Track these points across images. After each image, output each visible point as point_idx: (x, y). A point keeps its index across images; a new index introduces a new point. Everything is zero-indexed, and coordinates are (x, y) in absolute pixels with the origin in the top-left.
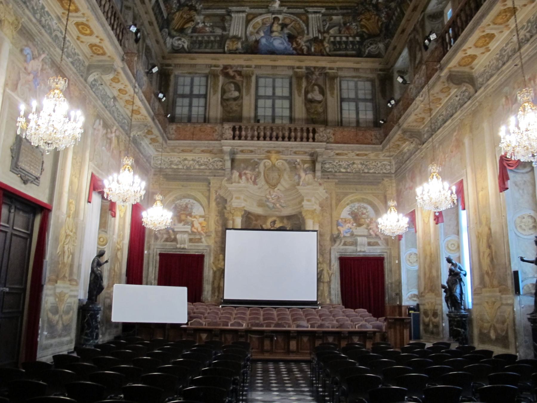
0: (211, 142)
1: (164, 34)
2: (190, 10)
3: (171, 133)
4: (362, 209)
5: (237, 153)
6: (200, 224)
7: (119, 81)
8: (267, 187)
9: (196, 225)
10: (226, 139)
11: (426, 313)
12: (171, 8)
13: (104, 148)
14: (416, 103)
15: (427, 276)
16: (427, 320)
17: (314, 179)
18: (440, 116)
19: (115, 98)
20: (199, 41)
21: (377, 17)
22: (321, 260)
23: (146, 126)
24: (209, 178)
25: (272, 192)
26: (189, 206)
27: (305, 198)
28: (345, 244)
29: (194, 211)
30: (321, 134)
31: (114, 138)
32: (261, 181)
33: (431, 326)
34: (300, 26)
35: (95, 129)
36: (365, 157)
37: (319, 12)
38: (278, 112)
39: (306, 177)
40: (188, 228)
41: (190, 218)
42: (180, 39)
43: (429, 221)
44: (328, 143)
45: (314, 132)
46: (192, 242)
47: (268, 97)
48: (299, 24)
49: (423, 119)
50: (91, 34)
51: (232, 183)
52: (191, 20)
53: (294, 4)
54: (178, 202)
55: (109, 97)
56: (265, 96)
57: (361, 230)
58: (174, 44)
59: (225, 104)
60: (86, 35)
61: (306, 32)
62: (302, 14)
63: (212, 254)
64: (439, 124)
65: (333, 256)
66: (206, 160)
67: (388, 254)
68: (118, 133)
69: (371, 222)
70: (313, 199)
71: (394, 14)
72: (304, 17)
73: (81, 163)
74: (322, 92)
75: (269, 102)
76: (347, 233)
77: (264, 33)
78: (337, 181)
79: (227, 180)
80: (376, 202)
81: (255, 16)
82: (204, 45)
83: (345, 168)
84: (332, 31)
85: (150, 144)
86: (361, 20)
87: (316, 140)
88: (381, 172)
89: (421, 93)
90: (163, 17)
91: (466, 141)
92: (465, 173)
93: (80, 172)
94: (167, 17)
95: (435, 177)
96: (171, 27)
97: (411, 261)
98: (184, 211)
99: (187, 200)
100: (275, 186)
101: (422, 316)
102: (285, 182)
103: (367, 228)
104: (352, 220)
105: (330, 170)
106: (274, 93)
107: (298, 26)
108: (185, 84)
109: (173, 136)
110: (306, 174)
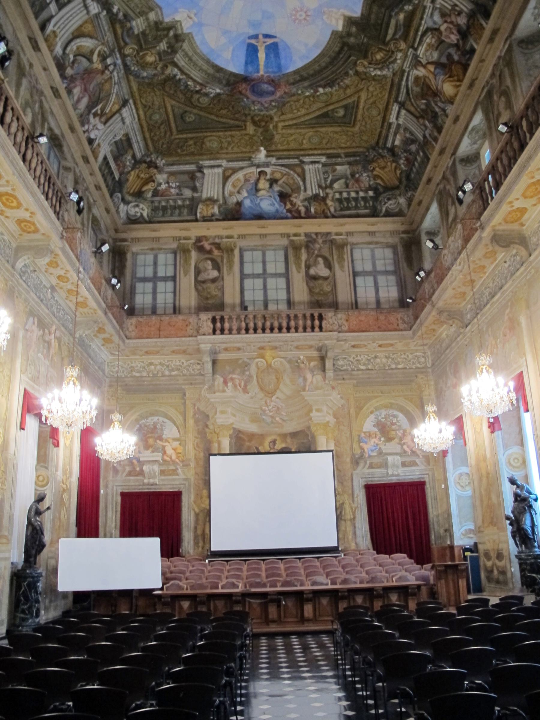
0: (183, 339)
1: (116, 200)
2: (149, 167)
3: (130, 329)
4: (391, 418)
5: (220, 352)
6: (175, 449)
7: (58, 265)
8: (261, 395)
9: (169, 451)
10: (204, 335)
11: (487, 555)
12: (124, 166)
13: (40, 354)
14: (452, 274)
15: (485, 503)
16: (489, 564)
17: (325, 381)
18: (485, 289)
19: (53, 288)
20: (163, 207)
21: (394, 165)
22: (340, 490)
23: (95, 322)
24: (183, 387)
25: (268, 401)
26: (158, 426)
27: (314, 408)
28: (371, 467)
29: (165, 432)
30: (330, 320)
31: (53, 341)
32: (254, 387)
33: (496, 572)
34: (294, 180)
35: (27, 330)
36: (390, 348)
37: (318, 162)
38: (272, 295)
39: (314, 379)
40: (158, 456)
41: (161, 443)
42: (137, 206)
43: (481, 429)
44: (339, 332)
45: (321, 318)
46: (165, 475)
47: (258, 276)
48: (292, 178)
49: (464, 293)
50: (19, 205)
51: (215, 393)
52: (151, 179)
53: (285, 153)
54: (143, 421)
55: (45, 287)
56: (253, 274)
57: (392, 447)
58: (129, 212)
59: (200, 288)
60: (12, 208)
61: (302, 188)
62: (296, 165)
63: (192, 490)
64: (485, 300)
65: (356, 484)
66: (178, 363)
67: (431, 476)
68: (58, 334)
69: (404, 435)
70: (325, 408)
71: (416, 159)
72: (299, 170)
73: (10, 377)
74: (329, 265)
75: (259, 282)
76: (372, 451)
77: (247, 191)
78: (355, 382)
79: (207, 389)
80: (410, 407)
81: (235, 171)
82: (169, 211)
83: (364, 364)
84: (336, 186)
85: (103, 345)
86: (374, 169)
87: (324, 330)
88: (414, 367)
89: (459, 260)
90: (114, 178)
91: (523, 320)
92: (525, 363)
93: (9, 388)
94: (120, 179)
95: (484, 371)
96: (125, 191)
97: (462, 484)
98: (151, 433)
99: (155, 419)
100: (270, 394)
101: (483, 560)
102: (286, 389)
103: (399, 444)
104: (378, 433)
105: (345, 368)
106: (265, 270)
107: (291, 182)
108: (147, 263)
109: (133, 334)
110: (313, 376)
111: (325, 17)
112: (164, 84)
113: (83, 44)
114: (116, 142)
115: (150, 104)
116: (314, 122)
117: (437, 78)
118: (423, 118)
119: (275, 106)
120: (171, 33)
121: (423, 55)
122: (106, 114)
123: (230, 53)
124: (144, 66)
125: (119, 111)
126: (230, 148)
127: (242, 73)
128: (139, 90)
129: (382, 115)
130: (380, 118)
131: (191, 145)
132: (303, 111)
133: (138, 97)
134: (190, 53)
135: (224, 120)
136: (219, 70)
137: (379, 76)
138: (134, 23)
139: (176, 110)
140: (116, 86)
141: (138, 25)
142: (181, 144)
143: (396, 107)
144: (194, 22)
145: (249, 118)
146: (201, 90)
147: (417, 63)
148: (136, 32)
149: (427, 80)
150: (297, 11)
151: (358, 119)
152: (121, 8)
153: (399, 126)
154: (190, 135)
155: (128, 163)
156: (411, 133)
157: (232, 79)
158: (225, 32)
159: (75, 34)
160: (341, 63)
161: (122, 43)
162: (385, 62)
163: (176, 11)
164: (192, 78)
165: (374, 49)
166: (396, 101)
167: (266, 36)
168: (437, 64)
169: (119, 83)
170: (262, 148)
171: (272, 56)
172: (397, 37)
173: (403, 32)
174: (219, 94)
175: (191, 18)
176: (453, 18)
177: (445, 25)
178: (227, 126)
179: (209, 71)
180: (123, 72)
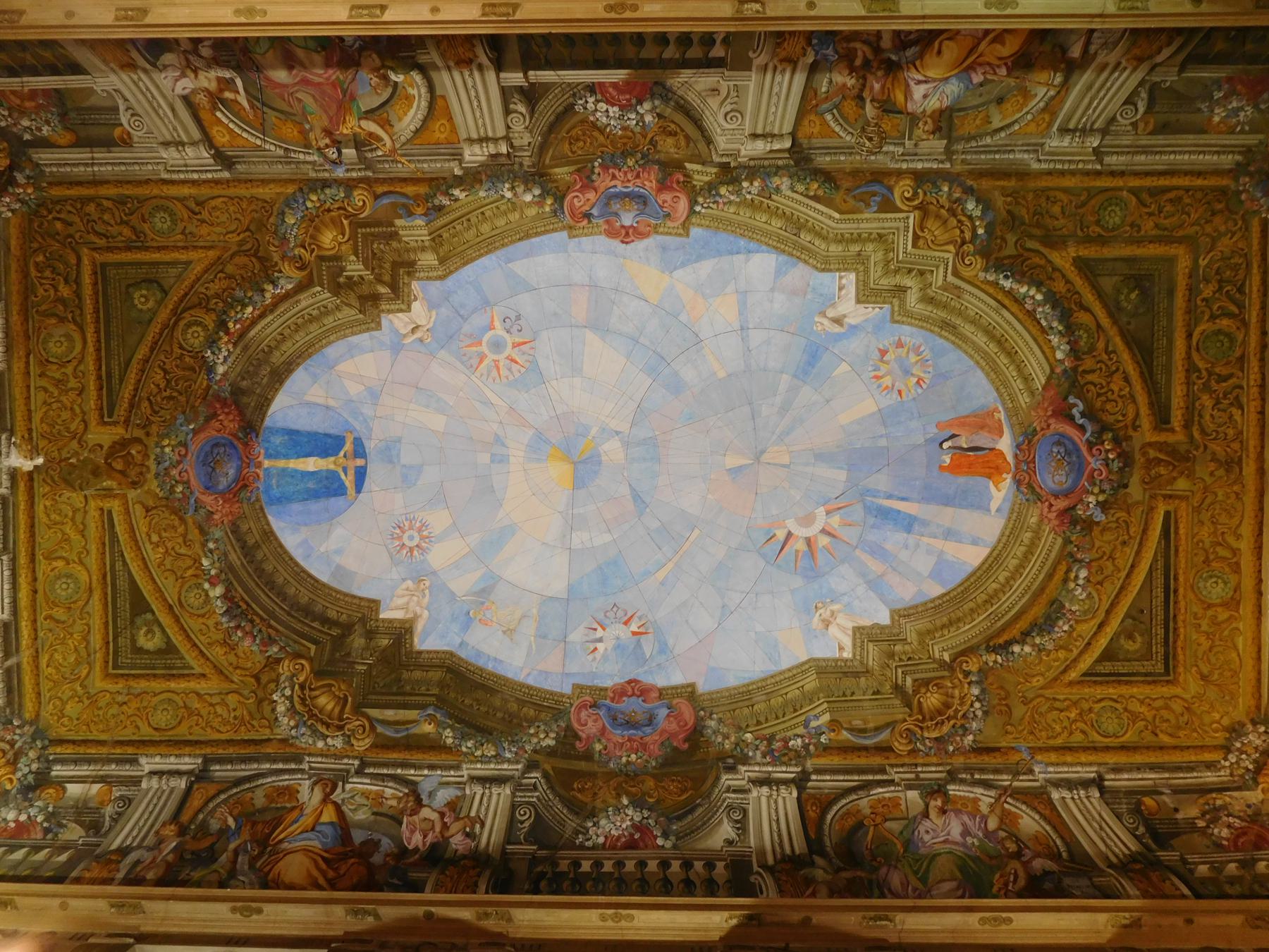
53: (22, 518)
71: (37, 849)
111: (409, 583)
112: (255, 255)
113: (412, 111)
114: (116, 109)
115: (205, 215)
116: (122, 584)
117: (310, 835)
118: (182, 831)
119: (172, 491)
120: (383, 290)
121: (352, 790)
122: (215, 108)
123: (321, 401)
124: (313, 222)
125: (208, 140)
126: (43, 382)
127: (268, 422)
128: (253, 199)
129: (157, 736)
130: (146, 732)
131: (56, 290)
132: (154, 556)
133: (231, 192)
134: (329, 321)
135: (132, 376)
136: (279, 376)
137: (274, 710)
139: (173, 271)
140: (281, 152)
141: (414, 230)
143: (189, 763)
144: (405, 336)
145: (138, 433)
146: (227, 332)
147: (329, 783)
149: (295, 814)
150: (420, 530)
151: (132, 683)
152: (458, 204)
153: (136, 781)
154: (87, 291)
155: (26, 123)
156: (117, 818)
157: (250, 401)
158: (374, 396)
159: (440, 102)
160: (298, 626)
161: (380, 189)
162: (312, 716)
163: (432, 306)
165: (341, 688)
166: (207, 761)
167: (361, 475)
168: (343, 826)
169: (286, 160)
170: (40, 461)
171: (311, 485)
172: (380, 729)
173: (395, 739)
174: (211, 370)
175: (413, 330)
176: (455, 827)
177: (434, 816)
178: (116, 380)
179: (277, 354)
180: (313, 175)
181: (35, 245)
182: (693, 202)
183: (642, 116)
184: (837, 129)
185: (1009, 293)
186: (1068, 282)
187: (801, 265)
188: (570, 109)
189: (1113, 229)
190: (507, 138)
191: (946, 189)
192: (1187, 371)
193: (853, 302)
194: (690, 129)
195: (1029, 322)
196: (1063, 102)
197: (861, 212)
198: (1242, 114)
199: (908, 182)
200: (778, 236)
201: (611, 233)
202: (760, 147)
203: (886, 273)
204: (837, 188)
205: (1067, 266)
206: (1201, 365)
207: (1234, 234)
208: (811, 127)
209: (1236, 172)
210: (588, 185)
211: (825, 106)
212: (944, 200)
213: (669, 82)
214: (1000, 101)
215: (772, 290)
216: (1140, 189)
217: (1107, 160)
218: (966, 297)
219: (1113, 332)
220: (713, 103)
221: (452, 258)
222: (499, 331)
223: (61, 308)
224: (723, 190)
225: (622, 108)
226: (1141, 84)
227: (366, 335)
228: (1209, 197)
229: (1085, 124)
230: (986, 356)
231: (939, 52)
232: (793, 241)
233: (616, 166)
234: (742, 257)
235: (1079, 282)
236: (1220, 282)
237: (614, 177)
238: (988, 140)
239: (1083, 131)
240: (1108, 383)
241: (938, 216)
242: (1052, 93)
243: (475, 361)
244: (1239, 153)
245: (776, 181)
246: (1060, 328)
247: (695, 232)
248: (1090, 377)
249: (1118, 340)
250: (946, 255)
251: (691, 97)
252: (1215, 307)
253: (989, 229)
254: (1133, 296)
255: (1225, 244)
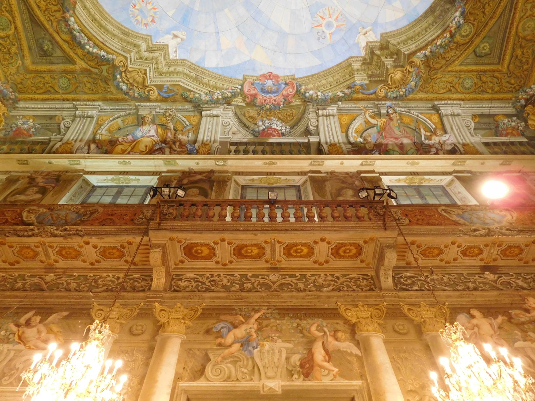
55: (473, 274)
90: (521, 143)
94: (527, 138)
112: (431, 68)
113: (355, 127)
115: (449, 86)
120: (378, 52)
122: (435, 129)
124: (403, 82)
131: (523, 52)
133: (435, 95)
134: (404, 37)
136: (431, 10)
138: (358, 82)
139: (468, 61)
140: (412, 112)
141: (361, 79)
142: (518, 63)
146: (451, 32)
148: (367, 82)
154: (509, 52)
155: (513, 124)
159: (344, 130)
164: (433, 40)
169: (410, 108)
174: (462, 14)
175: (366, 33)
178: (508, 8)
179: (430, 22)
180: (400, 102)
181: (526, 73)
182: (242, 89)
183: (263, 124)
184: (184, 119)
185: (101, 49)
186: (76, 54)
187: (194, 62)
188: (292, 127)
189: (62, 77)
190: (318, 116)
191: (136, 94)
192: (12, 11)
193: (170, 46)
194: (244, 120)
195: (90, 35)
196: (94, 128)
197: (170, 85)
198: (21, 123)
199: (152, 97)
200: (205, 75)
201: (276, 77)
202: (215, 112)
203: (156, 58)
204: (182, 95)
205: (78, 61)
206: (6, 14)
207: (10, 74)
208: (195, 120)
209: (17, 100)
210: (286, 98)
211: (189, 128)
212: (136, 90)
213: (252, 137)
214: (119, 129)
215: (206, 51)
216: (54, 94)
217: (71, 106)
218: (120, 47)
219: (51, 30)
220: (234, 129)
221: (347, 65)
222: (328, 32)
223: (523, 44)
224: (229, 94)
225: (271, 128)
226: (64, 135)
227: (388, 30)
228: (25, 90)
229: (83, 120)
230: (106, 19)
231: (146, 147)
232: (198, 73)
233: (274, 105)
234: (220, 66)
235: (72, 54)
236: (10, 54)
237: (275, 100)
238: (122, 114)
239: (84, 117)
240: (47, 5)
241: (138, 83)
242: (99, 132)
243: (340, 17)
244: (18, 108)
245: (207, 98)
246: (75, 32)
247: (241, 77)
248: (56, 8)
249: (48, 27)
250: (131, 66)
251: (243, 131)
252: (8, 41)
253: (115, 78)
254: (46, 47)
255: (13, 70)
